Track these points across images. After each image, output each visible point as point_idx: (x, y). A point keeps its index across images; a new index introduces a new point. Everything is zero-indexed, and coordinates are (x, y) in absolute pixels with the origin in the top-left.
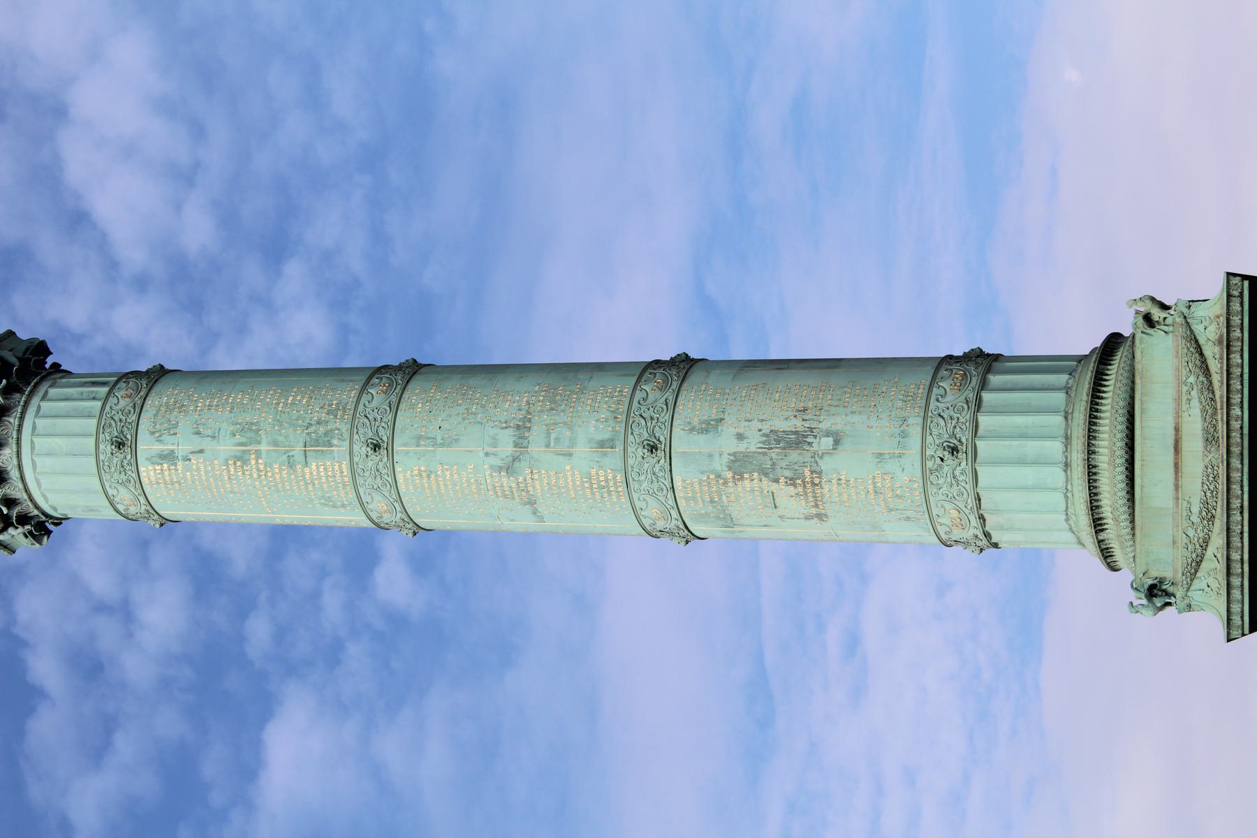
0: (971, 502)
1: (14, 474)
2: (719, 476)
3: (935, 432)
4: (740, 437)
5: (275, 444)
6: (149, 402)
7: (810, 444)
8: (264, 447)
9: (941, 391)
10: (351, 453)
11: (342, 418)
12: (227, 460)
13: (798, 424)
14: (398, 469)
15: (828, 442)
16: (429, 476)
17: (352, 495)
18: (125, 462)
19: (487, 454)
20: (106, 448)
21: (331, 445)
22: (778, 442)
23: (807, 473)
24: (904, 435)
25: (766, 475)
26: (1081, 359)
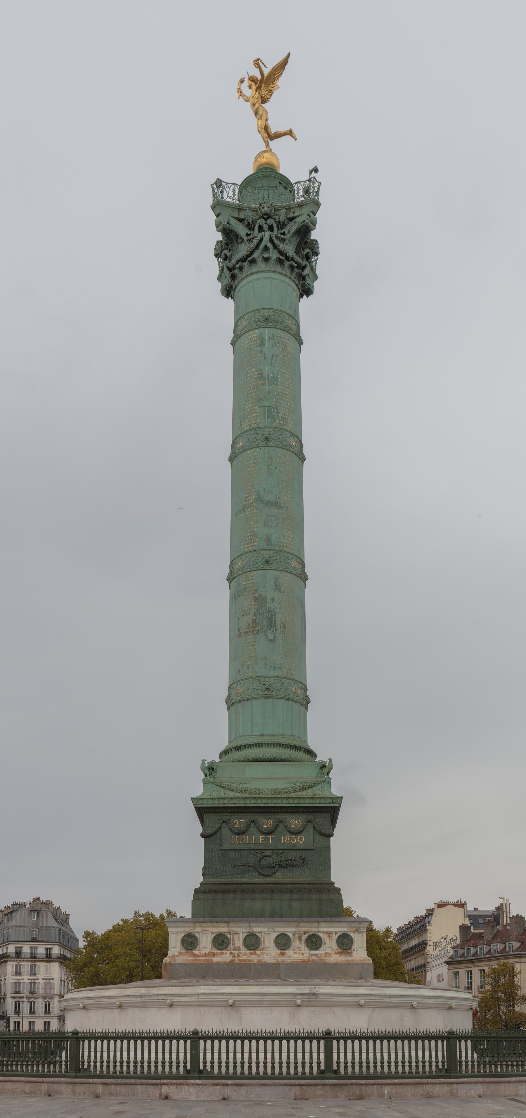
0: (246, 697)
1: (254, 269)
2: (256, 590)
3: (276, 681)
4: (273, 600)
5: (269, 393)
6: (287, 334)
7: (270, 629)
8: (267, 387)
9: (293, 684)
10: (264, 427)
11: (280, 423)
12: (261, 370)
13: (279, 624)
14: (258, 449)
15: (271, 637)
16: (255, 463)
17: (246, 429)
18: (260, 322)
19: (264, 489)
20: (266, 313)
21: (268, 418)
22: (271, 616)
23: (258, 628)
24: (274, 669)
25: (257, 611)
26: (306, 742)
